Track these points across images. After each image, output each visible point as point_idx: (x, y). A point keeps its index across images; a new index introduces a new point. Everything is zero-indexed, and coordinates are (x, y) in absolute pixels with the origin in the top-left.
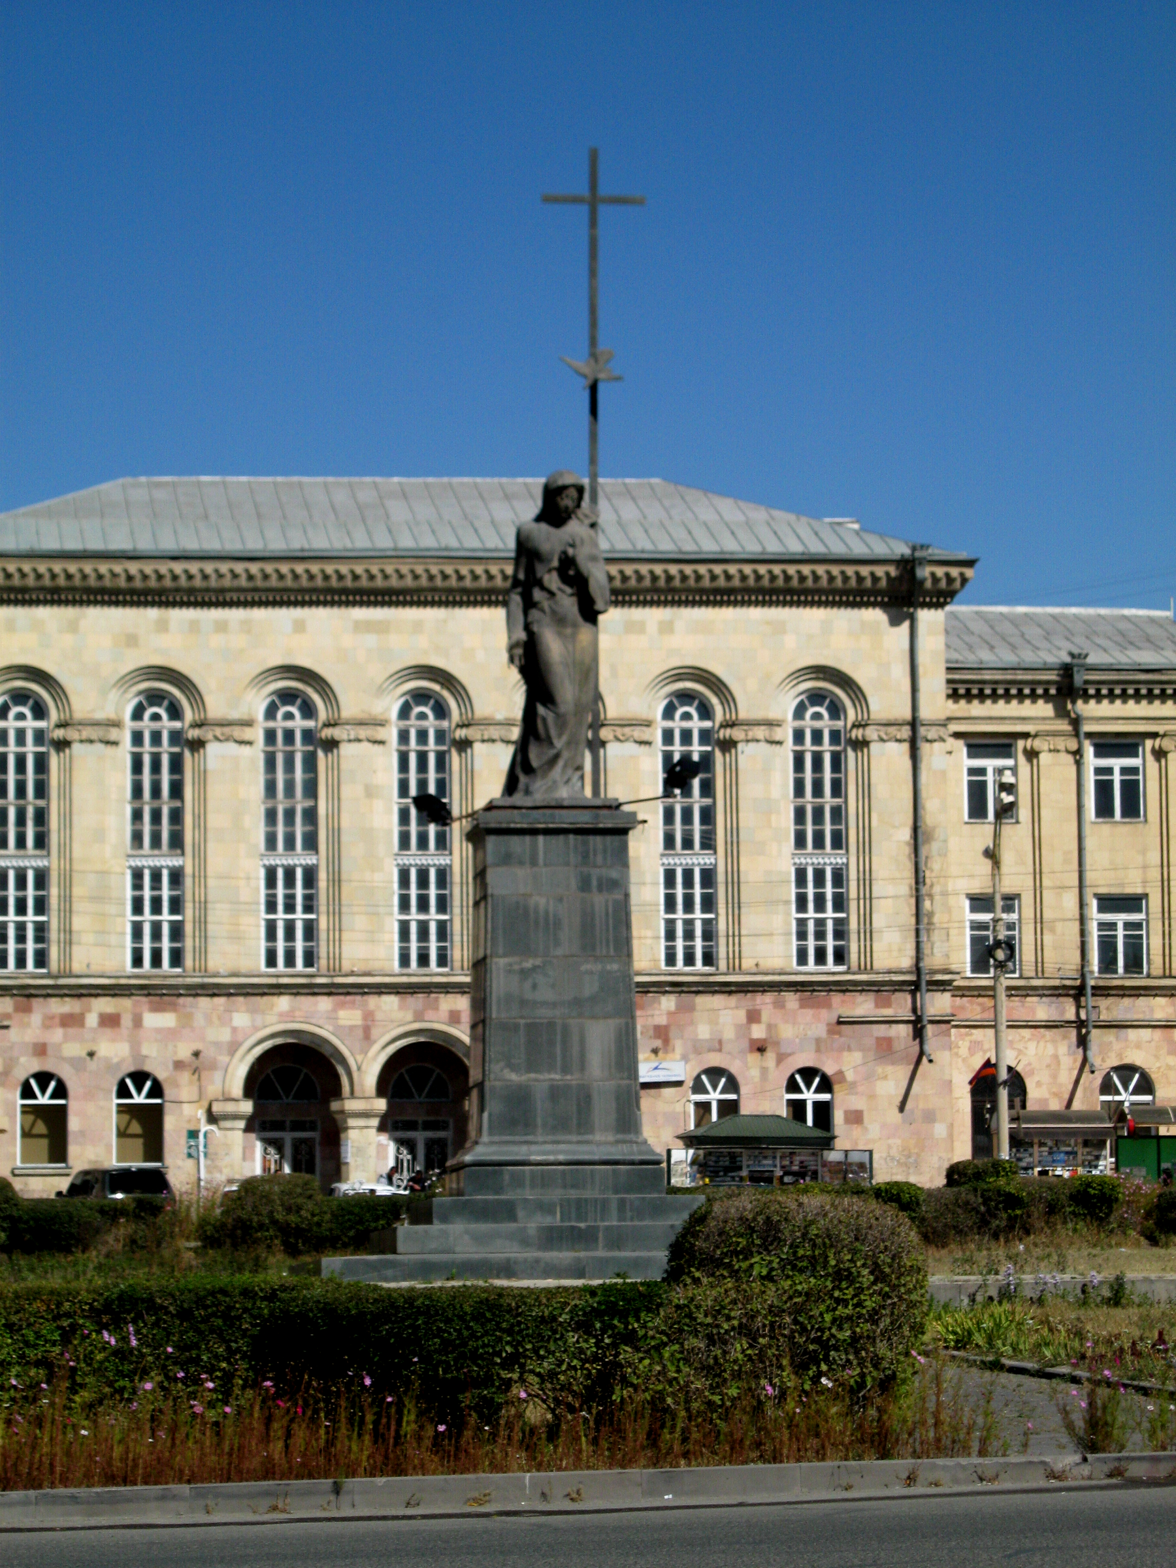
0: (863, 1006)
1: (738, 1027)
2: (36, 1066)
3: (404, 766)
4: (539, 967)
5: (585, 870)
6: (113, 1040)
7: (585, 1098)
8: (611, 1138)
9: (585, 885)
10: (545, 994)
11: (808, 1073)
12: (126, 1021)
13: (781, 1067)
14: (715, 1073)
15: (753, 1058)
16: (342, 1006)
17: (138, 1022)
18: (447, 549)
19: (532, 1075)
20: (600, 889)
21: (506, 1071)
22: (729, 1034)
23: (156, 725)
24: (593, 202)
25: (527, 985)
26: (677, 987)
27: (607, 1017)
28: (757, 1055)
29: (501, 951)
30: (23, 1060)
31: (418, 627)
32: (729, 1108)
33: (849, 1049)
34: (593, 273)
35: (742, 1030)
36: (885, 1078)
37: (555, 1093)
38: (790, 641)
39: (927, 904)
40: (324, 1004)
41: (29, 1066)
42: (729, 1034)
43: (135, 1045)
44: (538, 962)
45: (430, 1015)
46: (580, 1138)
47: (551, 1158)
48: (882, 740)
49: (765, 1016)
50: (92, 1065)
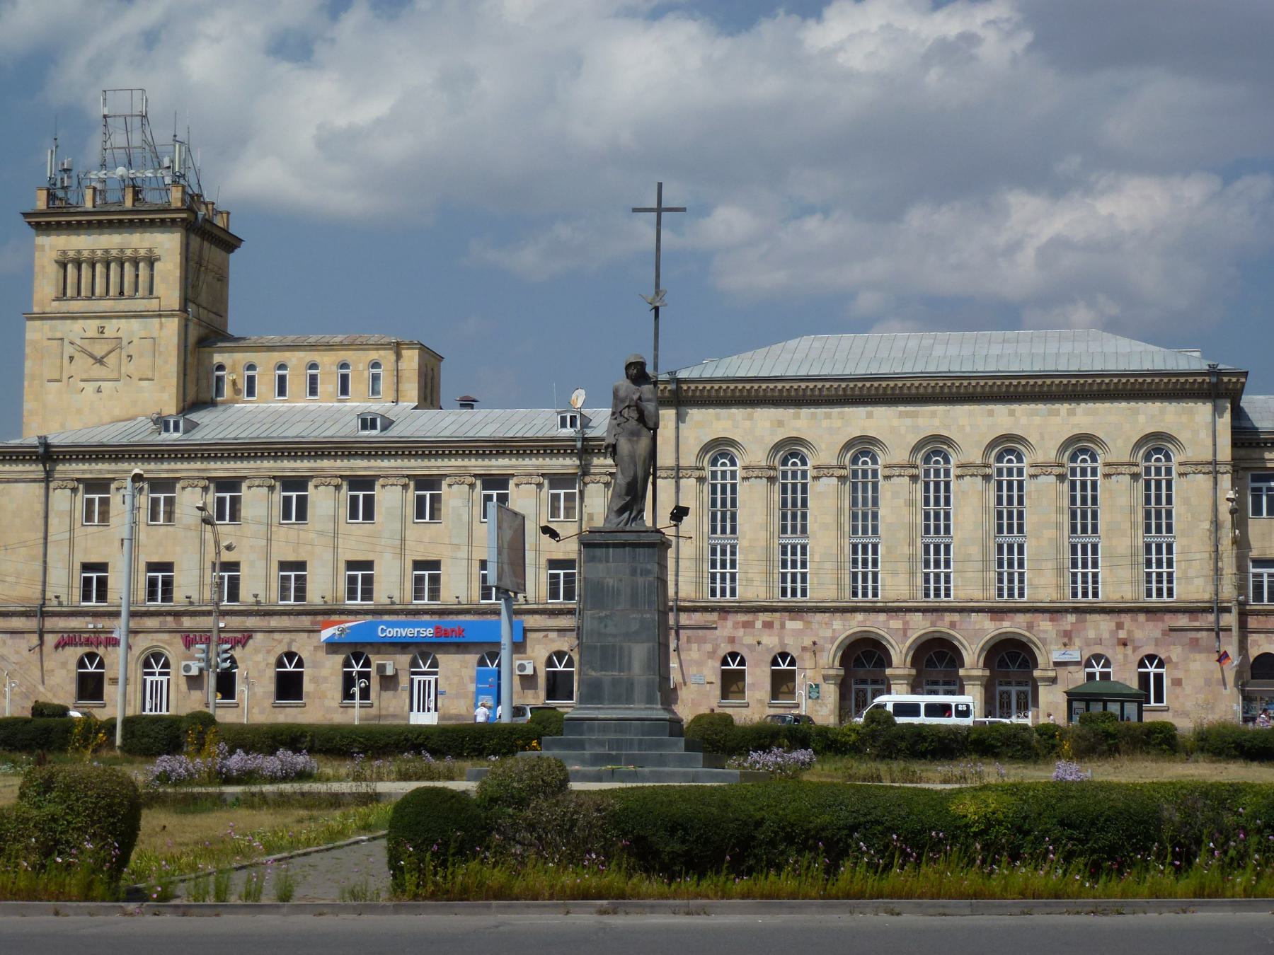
0: (1183, 621)
1: (1111, 632)
2: (729, 649)
3: (927, 489)
6: (770, 636)
7: (630, 685)
8: (643, 706)
9: (634, 572)
10: (611, 629)
11: (1151, 658)
12: (777, 625)
13: (1135, 654)
14: (1098, 657)
15: (1120, 649)
16: (892, 618)
17: (783, 626)
18: (950, 372)
19: (603, 673)
20: (641, 575)
21: (590, 671)
22: (1106, 635)
23: (794, 468)
24: (659, 210)
25: (602, 625)
26: (1076, 610)
27: (643, 642)
28: (1122, 647)
30: (722, 645)
31: (934, 415)
32: (1105, 676)
33: (1174, 644)
35: (1113, 633)
36: (1195, 661)
37: (615, 682)
38: (1142, 419)
39: (1220, 564)
40: (882, 617)
41: (725, 649)
42: (1106, 635)
43: (781, 638)
45: (939, 623)
46: (627, 706)
47: (609, 716)
48: (1194, 473)
49: (1126, 626)
50: (759, 648)
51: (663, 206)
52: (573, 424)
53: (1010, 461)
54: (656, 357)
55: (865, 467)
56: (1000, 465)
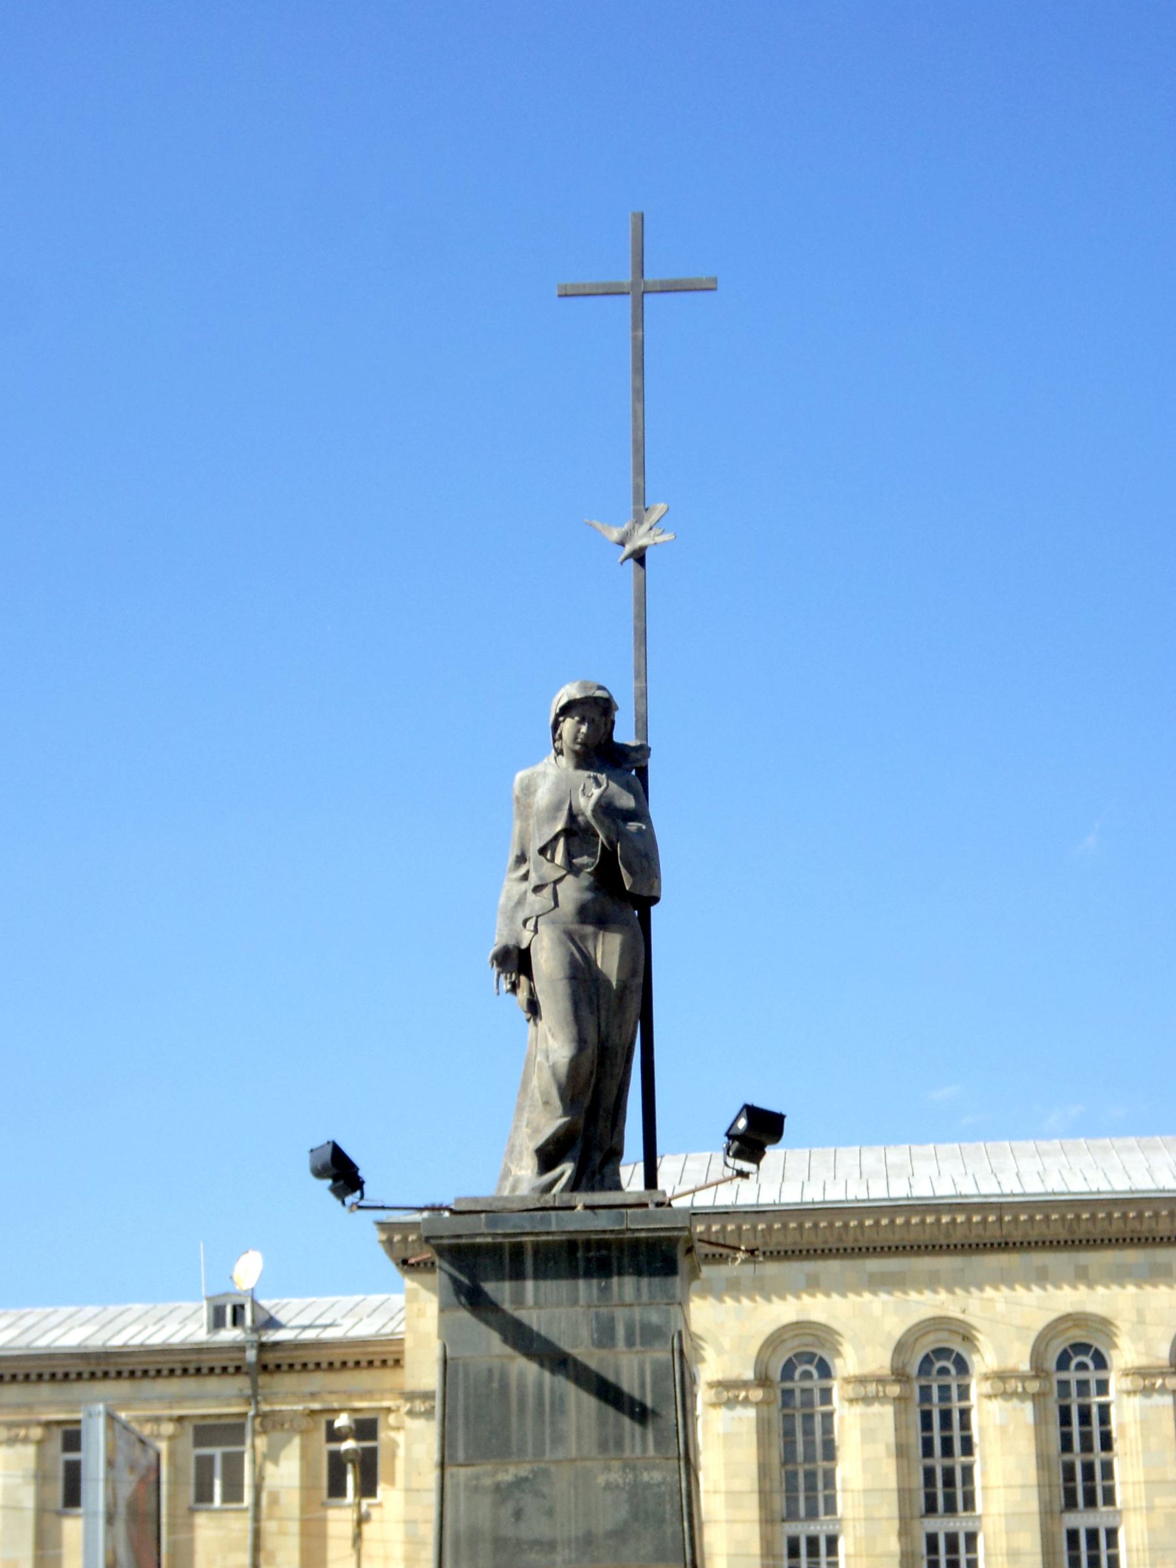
4: (526, 1479)
5: (604, 1310)
25: (507, 1510)
29: (461, 1455)
34: (639, 394)
44: (524, 1470)
51: (649, 276)
52: (237, 1320)
53: (1082, 1366)
54: (642, 695)
55: (807, 1384)
56: (1064, 1376)
